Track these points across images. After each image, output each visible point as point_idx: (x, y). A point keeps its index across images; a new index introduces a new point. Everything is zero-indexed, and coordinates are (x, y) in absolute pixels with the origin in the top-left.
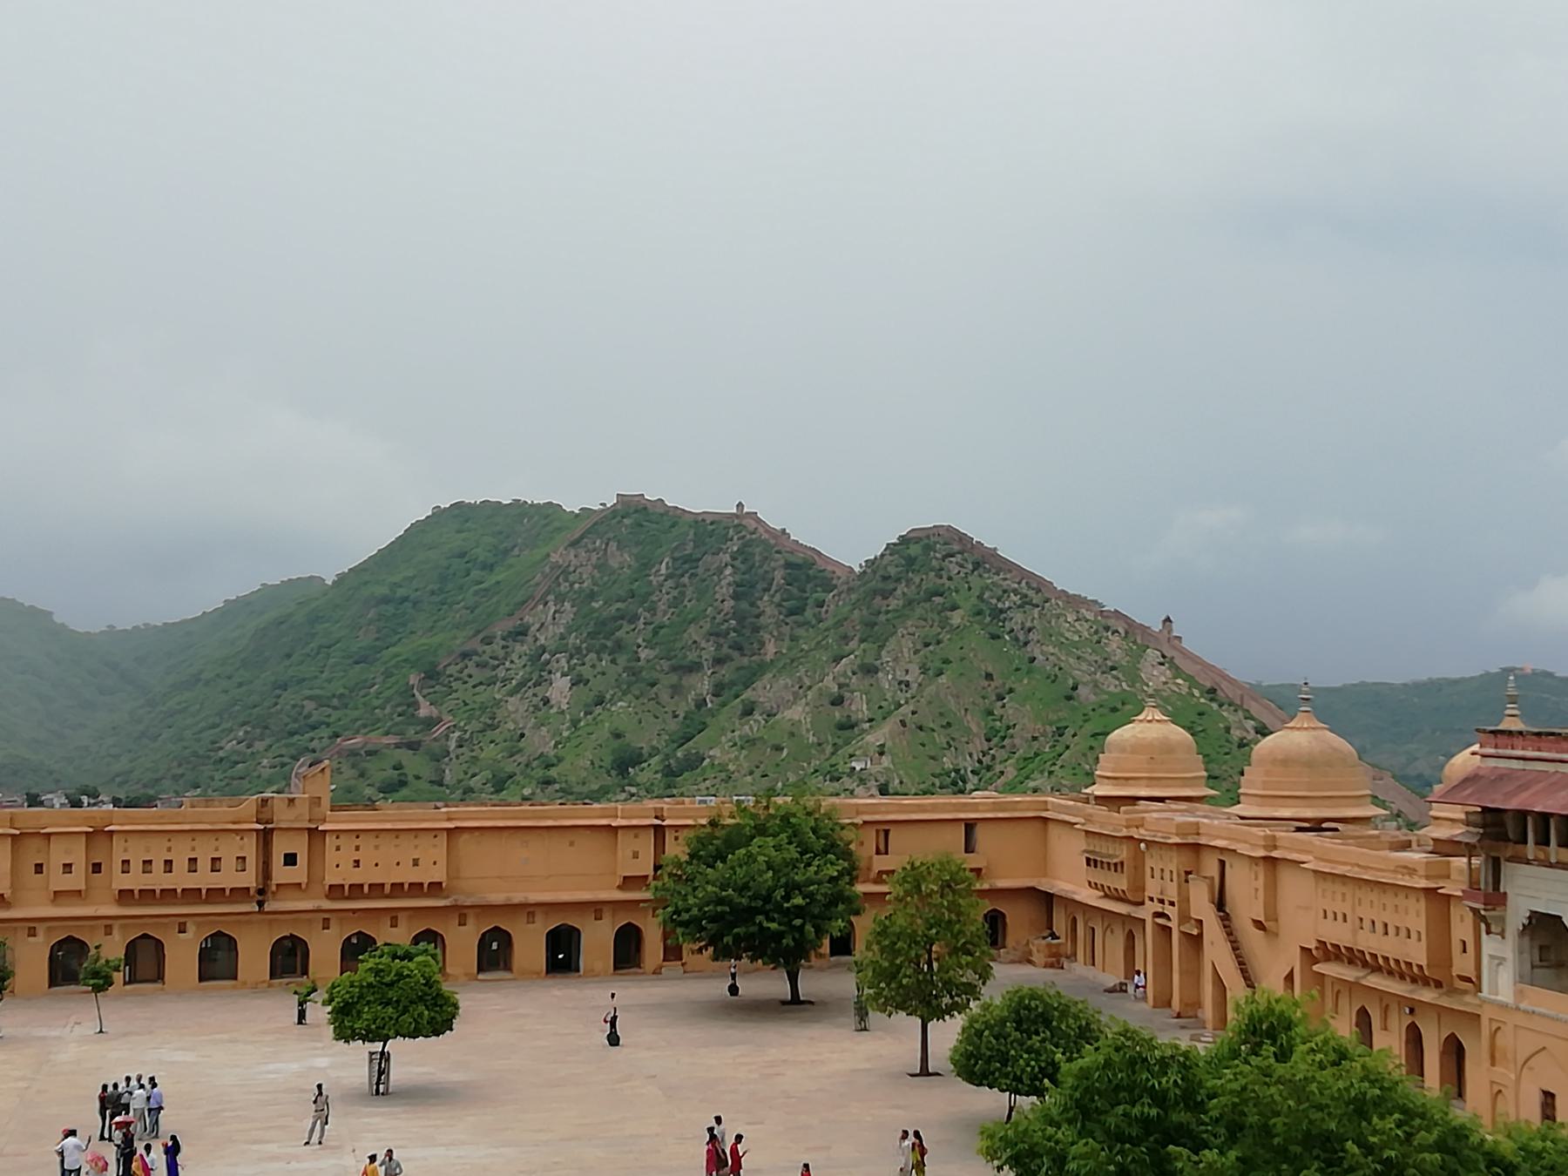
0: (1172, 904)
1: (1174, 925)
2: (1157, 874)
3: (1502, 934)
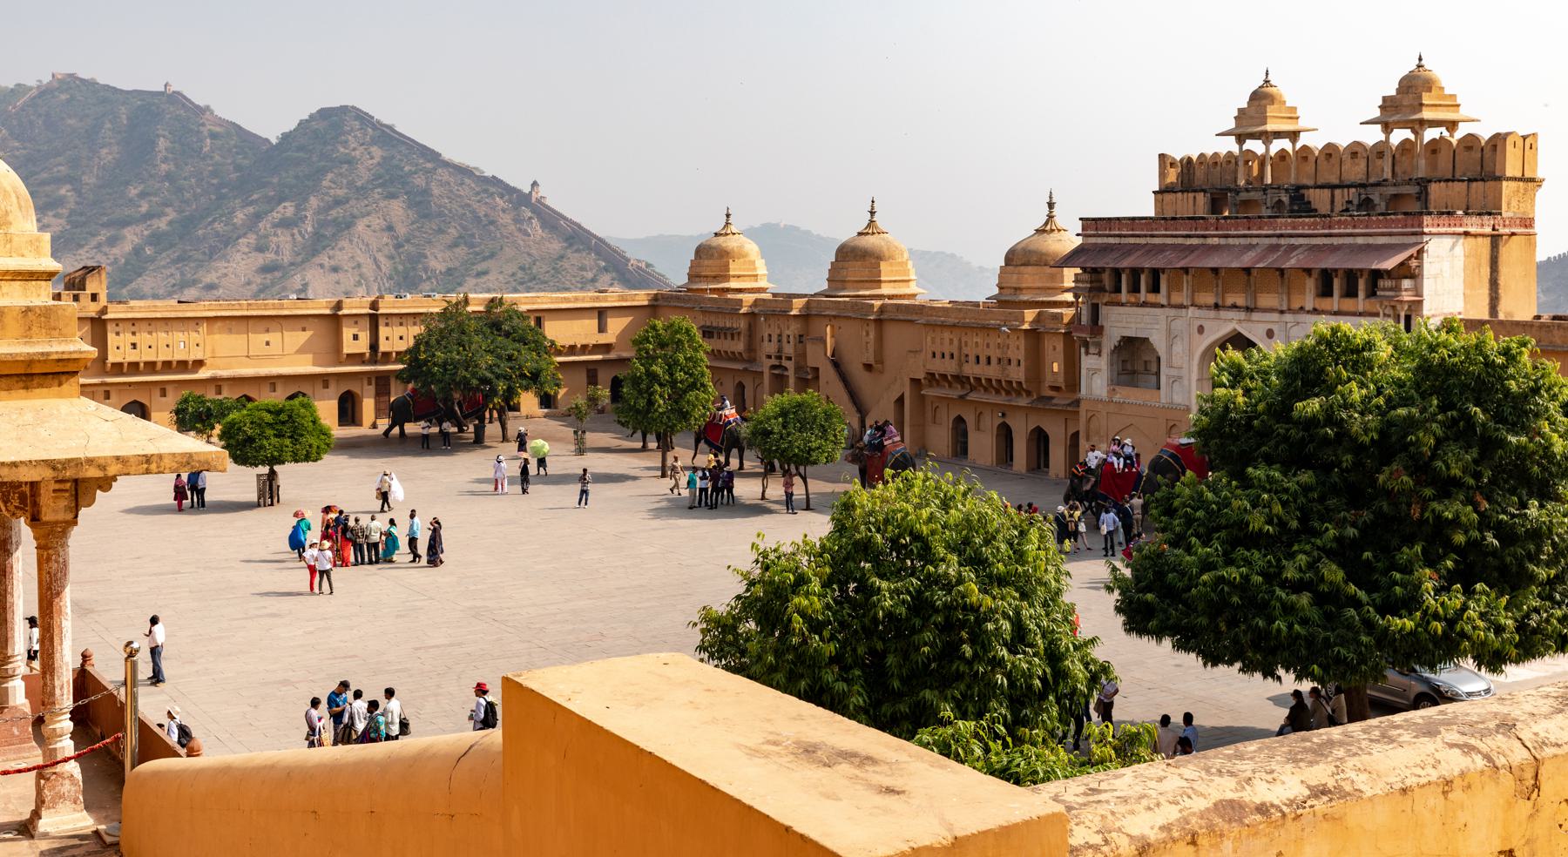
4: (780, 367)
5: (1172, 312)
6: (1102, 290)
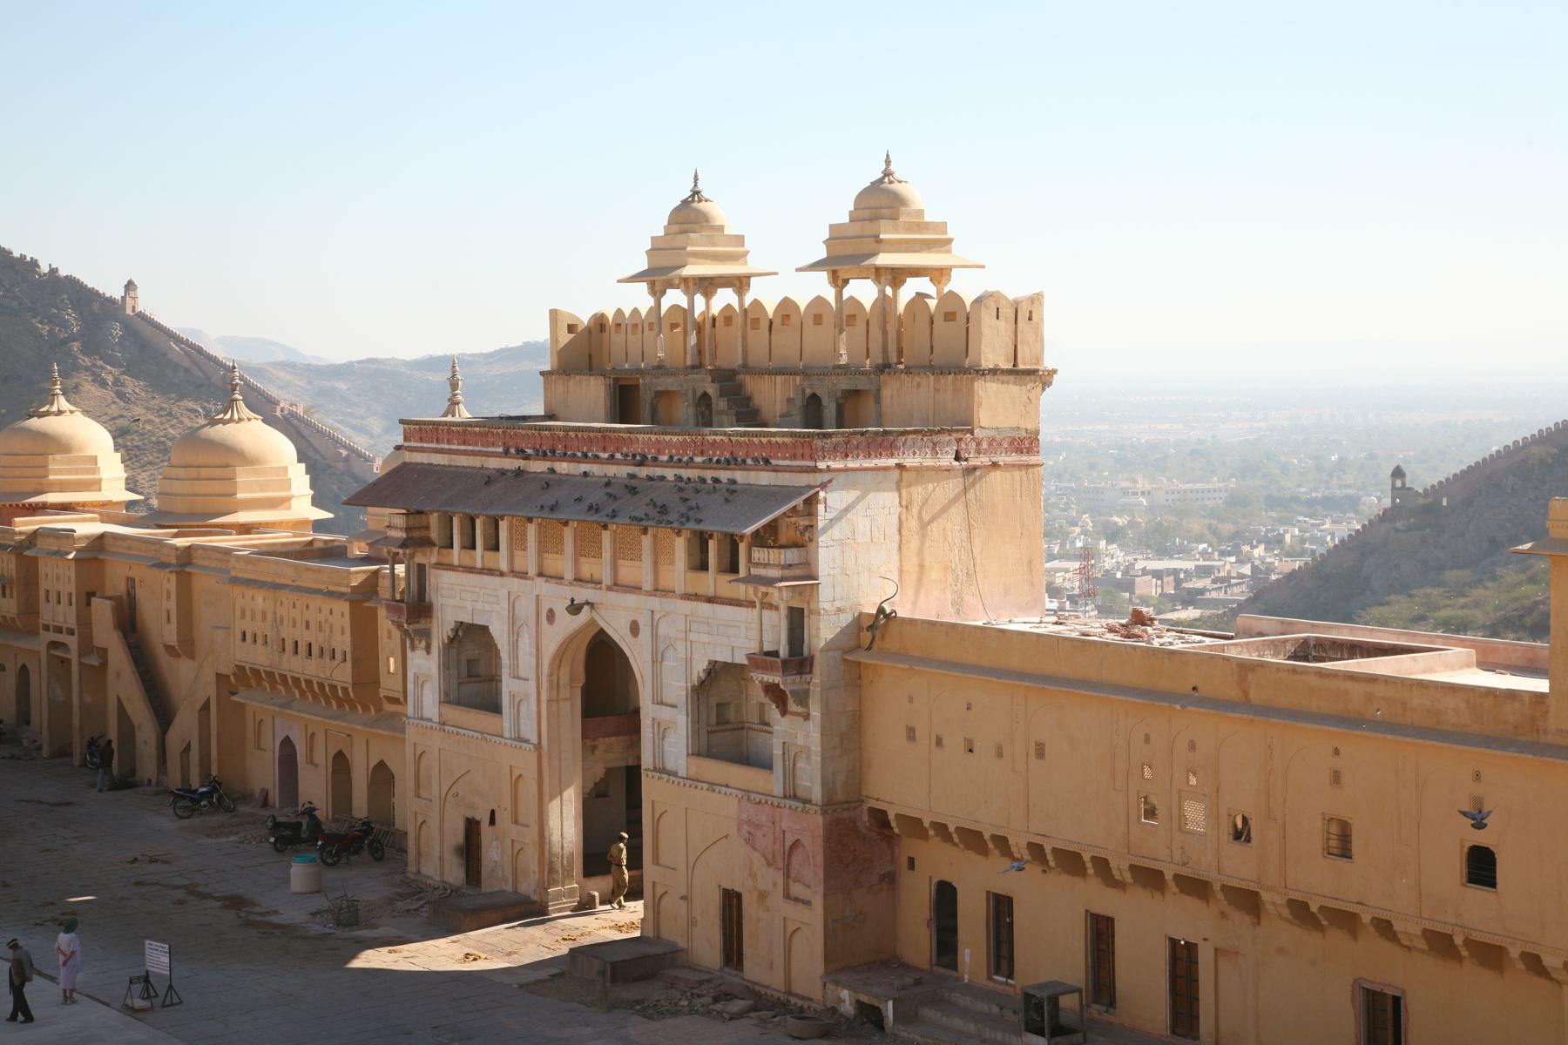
0: (71, 632)
1: (73, 655)
2: (53, 598)
3: (428, 649)
4: (54, 645)
5: (515, 583)
6: (427, 543)
